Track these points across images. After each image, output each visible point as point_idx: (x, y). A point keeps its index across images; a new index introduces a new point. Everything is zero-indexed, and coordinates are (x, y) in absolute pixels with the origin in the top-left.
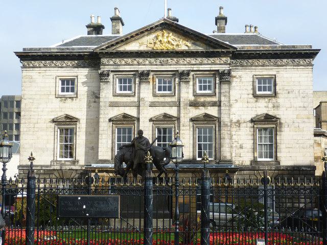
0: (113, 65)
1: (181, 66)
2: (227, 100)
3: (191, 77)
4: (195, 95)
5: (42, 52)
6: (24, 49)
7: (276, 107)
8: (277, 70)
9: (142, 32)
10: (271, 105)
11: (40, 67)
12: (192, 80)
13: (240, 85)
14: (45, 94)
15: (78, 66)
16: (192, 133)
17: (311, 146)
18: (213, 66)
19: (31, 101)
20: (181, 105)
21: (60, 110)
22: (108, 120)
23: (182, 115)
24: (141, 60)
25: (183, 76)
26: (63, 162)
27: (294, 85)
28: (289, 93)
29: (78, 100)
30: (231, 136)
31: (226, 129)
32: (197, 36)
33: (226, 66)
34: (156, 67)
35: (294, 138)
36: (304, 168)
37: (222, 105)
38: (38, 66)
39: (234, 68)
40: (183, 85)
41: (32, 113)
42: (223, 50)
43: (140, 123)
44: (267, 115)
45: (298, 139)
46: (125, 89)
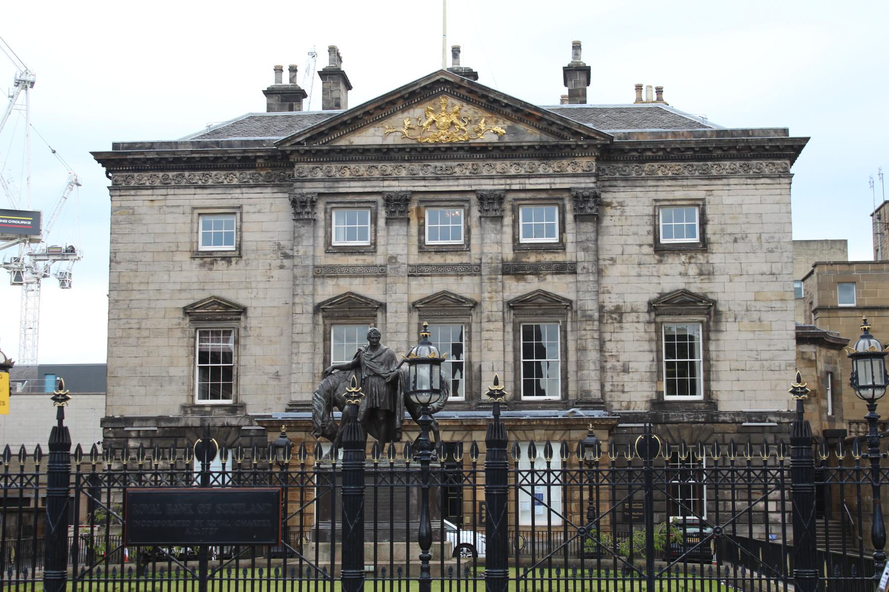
2: (591, 258)
3: (507, 206)
4: (517, 246)
5: (158, 153)
6: (115, 146)
7: (706, 274)
9: (393, 103)
10: (693, 270)
11: (153, 188)
14: (164, 251)
16: (510, 337)
17: (790, 365)
18: (558, 180)
20: (483, 273)
21: (202, 288)
22: (310, 309)
23: (486, 295)
24: (389, 167)
26: (208, 409)
27: (748, 223)
28: (735, 241)
29: (242, 263)
30: (602, 343)
31: (588, 328)
32: (517, 110)
33: (588, 180)
34: (422, 183)
35: (750, 347)
37: (579, 270)
38: (148, 184)
39: (607, 183)
40: (489, 225)
41: (136, 295)
42: (580, 143)
43: (388, 314)
44: (685, 292)
45: (759, 349)
46: (351, 237)
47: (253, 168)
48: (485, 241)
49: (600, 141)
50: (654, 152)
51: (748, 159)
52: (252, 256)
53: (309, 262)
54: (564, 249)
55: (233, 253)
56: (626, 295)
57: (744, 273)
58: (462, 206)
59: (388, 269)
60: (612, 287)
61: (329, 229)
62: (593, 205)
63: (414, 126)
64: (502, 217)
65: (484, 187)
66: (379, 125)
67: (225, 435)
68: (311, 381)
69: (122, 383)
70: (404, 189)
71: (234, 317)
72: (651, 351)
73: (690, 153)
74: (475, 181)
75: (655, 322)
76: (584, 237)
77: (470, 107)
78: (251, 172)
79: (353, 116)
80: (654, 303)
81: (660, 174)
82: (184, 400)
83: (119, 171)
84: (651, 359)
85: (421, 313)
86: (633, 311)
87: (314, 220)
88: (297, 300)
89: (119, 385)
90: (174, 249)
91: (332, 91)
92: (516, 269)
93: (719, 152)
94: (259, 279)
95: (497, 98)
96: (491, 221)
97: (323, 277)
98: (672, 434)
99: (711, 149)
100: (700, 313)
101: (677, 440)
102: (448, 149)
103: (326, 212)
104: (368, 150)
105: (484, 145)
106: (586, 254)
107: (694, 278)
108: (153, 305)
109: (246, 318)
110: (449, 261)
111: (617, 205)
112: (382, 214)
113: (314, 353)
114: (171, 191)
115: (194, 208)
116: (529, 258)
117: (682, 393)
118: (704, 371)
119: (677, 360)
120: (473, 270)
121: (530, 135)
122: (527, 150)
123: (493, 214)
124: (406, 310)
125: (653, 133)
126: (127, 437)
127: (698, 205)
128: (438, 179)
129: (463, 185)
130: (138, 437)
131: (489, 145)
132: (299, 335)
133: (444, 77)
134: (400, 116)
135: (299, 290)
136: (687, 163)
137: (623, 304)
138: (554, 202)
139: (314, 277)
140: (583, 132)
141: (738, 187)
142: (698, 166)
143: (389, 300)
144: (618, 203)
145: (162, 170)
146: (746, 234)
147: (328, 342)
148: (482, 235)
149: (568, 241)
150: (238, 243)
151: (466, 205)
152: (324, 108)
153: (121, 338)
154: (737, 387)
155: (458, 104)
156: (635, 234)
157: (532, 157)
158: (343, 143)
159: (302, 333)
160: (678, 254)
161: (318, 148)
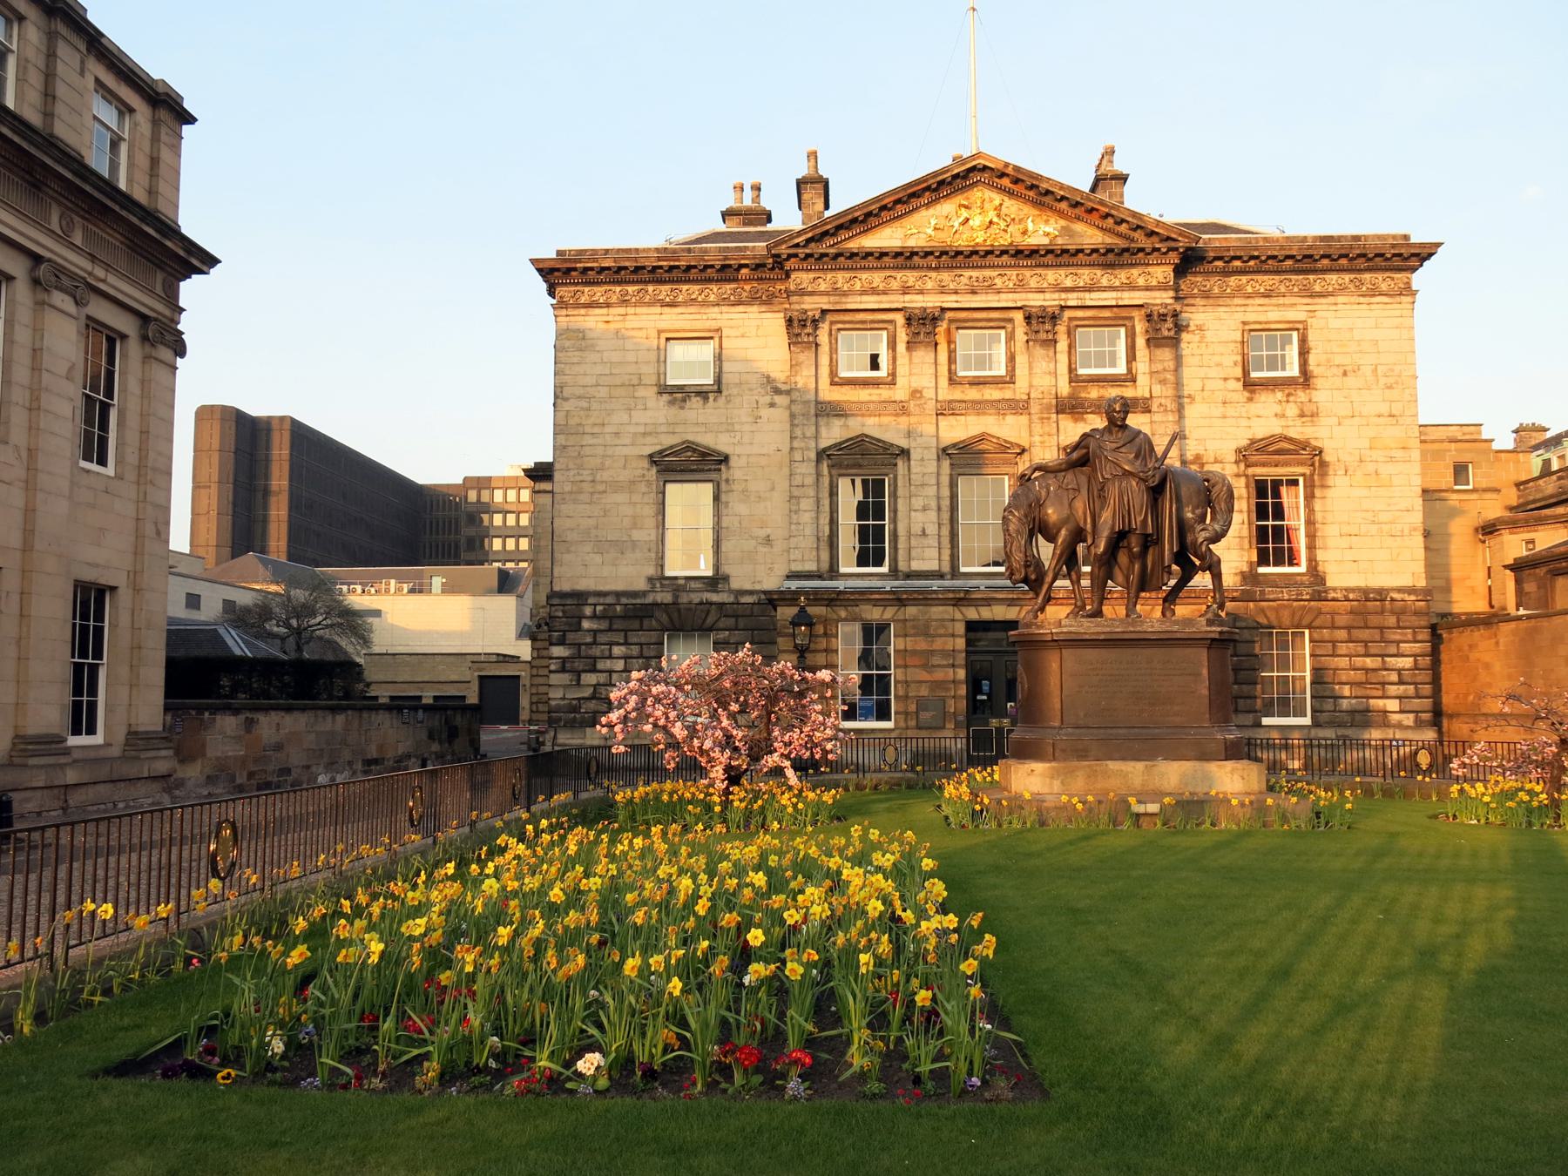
0: (822, 294)
1: (1031, 296)
2: (1170, 392)
3: (1061, 329)
4: (1074, 378)
6: (559, 253)
8: (1309, 308)
10: (1292, 410)
11: (608, 305)
12: (1065, 337)
14: (623, 385)
15: (723, 301)
17: (1415, 529)
18: (1126, 295)
19: (584, 404)
22: (813, 455)
23: (1037, 439)
24: (910, 277)
25: (1042, 323)
26: (682, 582)
27: (1360, 352)
28: (1345, 374)
29: (722, 401)
34: (954, 297)
36: (1396, 596)
37: (1154, 408)
40: (1039, 351)
41: (588, 440)
47: (735, 280)
49: (1182, 244)
51: (1360, 271)
58: (1003, 328)
64: (1056, 342)
65: (1032, 303)
66: (897, 224)
69: (573, 549)
73: (1289, 262)
75: (1247, 476)
76: (1159, 367)
77: (1013, 202)
78: (733, 286)
79: (865, 211)
81: (1249, 289)
82: (651, 571)
83: (566, 284)
86: (1216, 461)
87: (817, 345)
88: (796, 444)
89: (568, 552)
90: (635, 382)
92: (1074, 407)
93: (1326, 262)
94: (744, 419)
96: (1041, 346)
97: (828, 415)
98: (1269, 614)
100: (1302, 464)
101: (1275, 623)
103: (830, 334)
104: (886, 254)
108: (609, 452)
112: (902, 337)
114: (631, 310)
115: (663, 331)
117: (1278, 563)
118: (1307, 536)
120: (1019, 407)
121: (1089, 236)
122: (1089, 255)
123: (1043, 336)
125: (1240, 239)
126: (581, 617)
127: (1298, 329)
128: (974, 292)
129: (1005, 300)
130: (594, 616)
134: (924, 213)
135: (798, 432)
138: (1121, 322)
139: (817, 416)
140: (1161, 231)
145: (619, 283)
148: (1030, 363)
151: (1009, 326)
152: (803, 223)
153: (571, 493)
154: (1349, 555)
155: (997, 198)
156: (1218, 365)
158: (853, 245)
160: (1273, 390)
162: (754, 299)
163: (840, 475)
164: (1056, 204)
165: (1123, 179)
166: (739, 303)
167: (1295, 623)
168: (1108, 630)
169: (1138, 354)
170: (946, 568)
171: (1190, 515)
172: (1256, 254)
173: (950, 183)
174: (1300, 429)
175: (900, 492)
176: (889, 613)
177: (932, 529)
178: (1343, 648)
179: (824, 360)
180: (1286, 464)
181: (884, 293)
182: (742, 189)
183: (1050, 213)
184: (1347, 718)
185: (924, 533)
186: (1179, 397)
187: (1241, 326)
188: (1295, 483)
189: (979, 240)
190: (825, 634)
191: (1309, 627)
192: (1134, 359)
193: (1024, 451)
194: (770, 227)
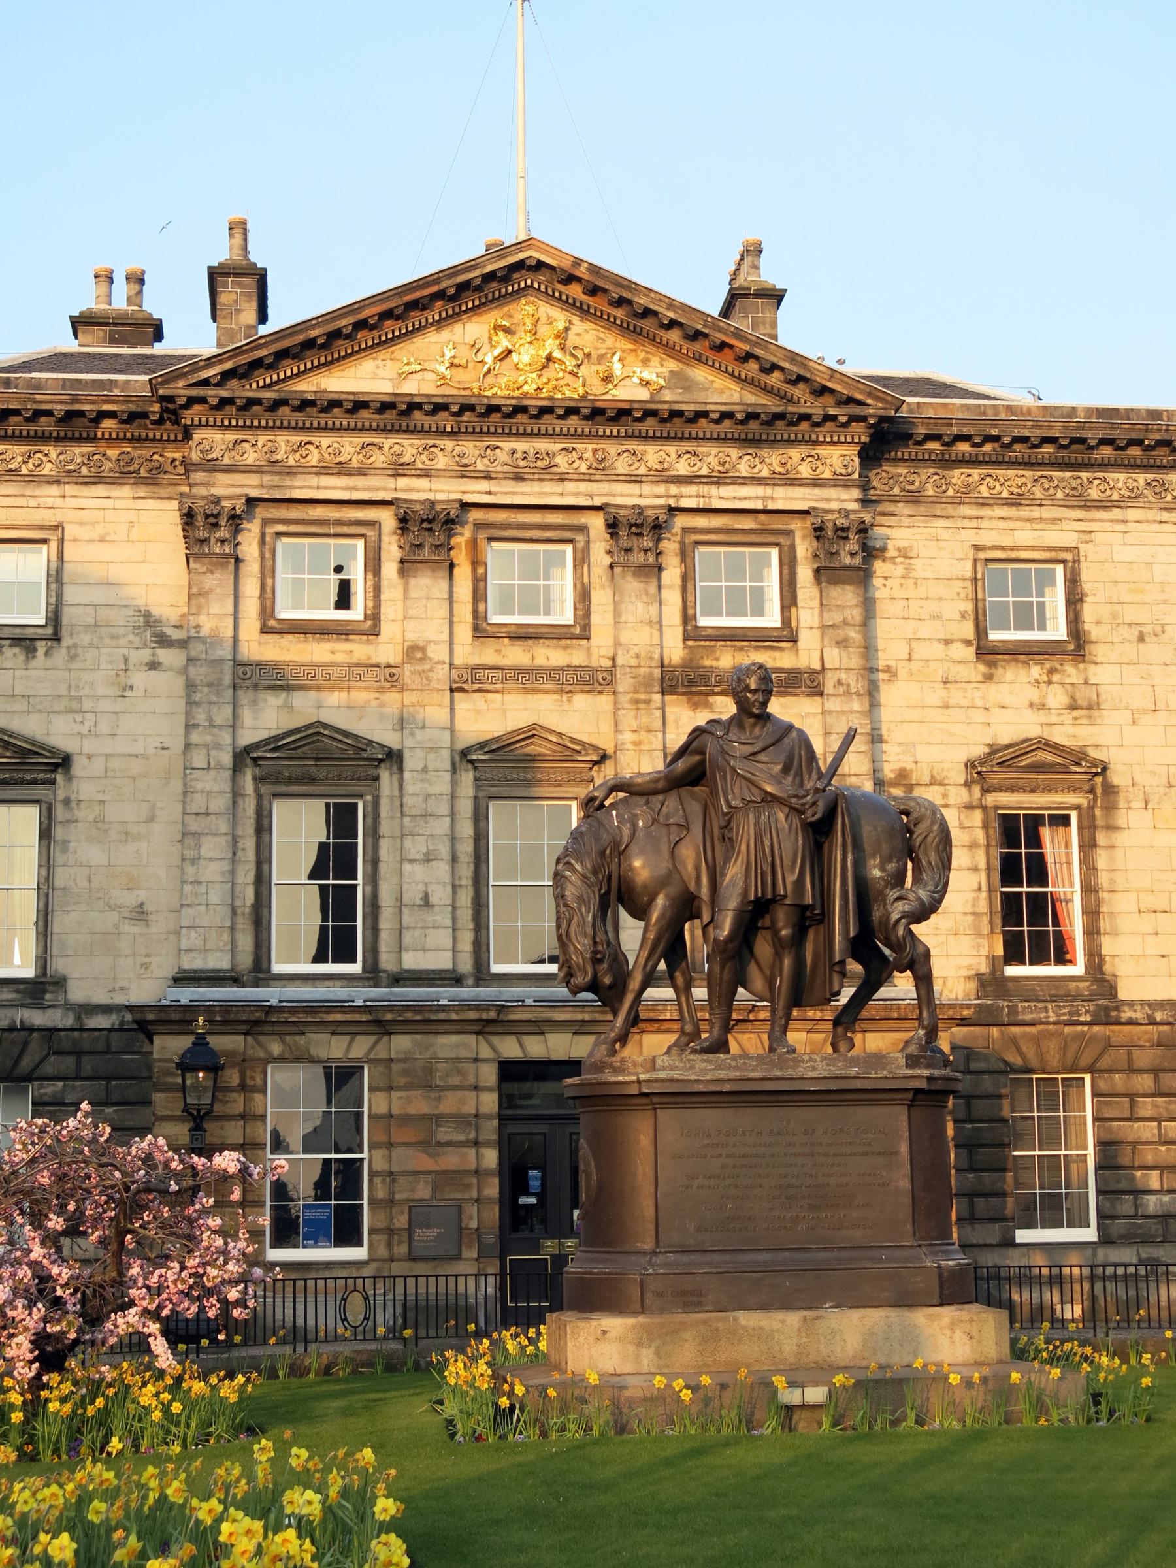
1: (618, 488)
3: (670, 546)
4: (691, 633)
10: (1057, 698)
13: (903, 594)
18: (780, 492)
20: (620, 689)
22: (227, 759)
23: (627, 737)
24: (408, 447)
27: (1165, 602)
28: (1141, 638)
29: (60, 655)
34: (484, 485)
37: (829, 688)
40: (631, 584)
42: (832, 412)
43: (407, 775)
47: (91, 439)
48: (623, 619)
49: (874, 409)
50: (975, 445)
51: (1161, 468)
52: (85, 639)
53: (226, 652)
54: (795, 641)
55: (40, 631)
56: (919, 747)
57: (1161, 706)
58: (570, 541)
59: (407, 673)
60: (889, 730)
61: (269, 581)
62: (857, 548)
63: (463, 362)
64: (660, 568)
66: (385, 354)
67: (16, 1051)
68: (228, 924)
70: (441, 497)
71: (41, 776)
72: (975, 869)
73: (1048, 449)
74: (600, 485)
75: (984, 808)
76: (836, 617)
77: (588, 325)
78: (87, 449)
80: (982, 764)
81: (984, 491)
84: (976, 886)
85: (481, 774)
86: (933, 782)
87: (238, 560)
88: (195, 738)
91: (238, 311)
92: (691, 683)
93: (1107, 450)
94: (100, 691)
95: (652, 307)
96: (635, 574)
97: (256, 687)
98: (1024, 1048)
99: (1093, 443)
100: (1073, 788)
101: (1034, 1062)
102: (544, 411)
103: (262, 542)
104: (364, 405)
105: (626, 406)
106: (844, 654)
107: (1060, 715)
109: (69, 779)
110: (541, 661)
111: (895, 554)
112: (392, 551)
113: (234, 861)
116: (717, 659)
117: (1039, 958)
119: (1025, 889)
123: (638, 558)
124: (447, 765)
125: (968, 407)
127: (1063, 561)
128: (519, 478)
129: (574, 493)
131: (636, 406)
132: (199, 818)
133: (537, 255)
135: (200, 716)
136: (1039, 473)
137: (913, 766)
138: (771, 539)
139: (235, 687)
140: (838, 387)
141: (1143, 527)
142: (1061, 480)
143: (408, 743)
144: (899, 550)
146: (1163, 625)
147: (265, 837)
148: (616, 604)
149: (802, 624)
150: (52, 608)
151: (580, 539)
152: (219, 345)
154: (1153, 946)
155: (560, 318)
157: (725, 439)
158: (307, 386)
159: (208, 814)
160: (1025, 662)
161: (250, 394)
162: (124, 475)
163: (276, 795)
164: (662, 333)
165: (776, 297)
166: (97, 480)
167: (1069, 1063)
168: (737, 1074)
169: (801, 595)
170: (466, 965)
171: (877, 873)
172: (994, 432)
173: (479, 289)
174: (1071, 730)
175: (385, 828)
176: (360, 1047)
177: (441, 896)
178: (1146, 1107)
179: (251, 588)
180: (1048, 789)
181: (361, 472)
182: (111, 280)
183: (650, 348)
184: (1155, 1227)
185: (426, 903)
186: (872, 670)
187: (971, 553)
188: (1065, 821)
189: (529, 388)
190: (243, 1087)
191: (1091, 1070)
192: (794, 602)
193: (604, 757)
194: (158, 349)
